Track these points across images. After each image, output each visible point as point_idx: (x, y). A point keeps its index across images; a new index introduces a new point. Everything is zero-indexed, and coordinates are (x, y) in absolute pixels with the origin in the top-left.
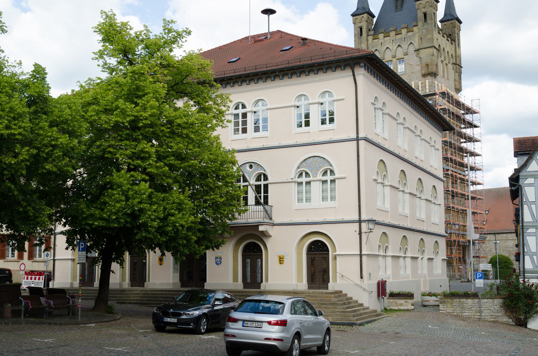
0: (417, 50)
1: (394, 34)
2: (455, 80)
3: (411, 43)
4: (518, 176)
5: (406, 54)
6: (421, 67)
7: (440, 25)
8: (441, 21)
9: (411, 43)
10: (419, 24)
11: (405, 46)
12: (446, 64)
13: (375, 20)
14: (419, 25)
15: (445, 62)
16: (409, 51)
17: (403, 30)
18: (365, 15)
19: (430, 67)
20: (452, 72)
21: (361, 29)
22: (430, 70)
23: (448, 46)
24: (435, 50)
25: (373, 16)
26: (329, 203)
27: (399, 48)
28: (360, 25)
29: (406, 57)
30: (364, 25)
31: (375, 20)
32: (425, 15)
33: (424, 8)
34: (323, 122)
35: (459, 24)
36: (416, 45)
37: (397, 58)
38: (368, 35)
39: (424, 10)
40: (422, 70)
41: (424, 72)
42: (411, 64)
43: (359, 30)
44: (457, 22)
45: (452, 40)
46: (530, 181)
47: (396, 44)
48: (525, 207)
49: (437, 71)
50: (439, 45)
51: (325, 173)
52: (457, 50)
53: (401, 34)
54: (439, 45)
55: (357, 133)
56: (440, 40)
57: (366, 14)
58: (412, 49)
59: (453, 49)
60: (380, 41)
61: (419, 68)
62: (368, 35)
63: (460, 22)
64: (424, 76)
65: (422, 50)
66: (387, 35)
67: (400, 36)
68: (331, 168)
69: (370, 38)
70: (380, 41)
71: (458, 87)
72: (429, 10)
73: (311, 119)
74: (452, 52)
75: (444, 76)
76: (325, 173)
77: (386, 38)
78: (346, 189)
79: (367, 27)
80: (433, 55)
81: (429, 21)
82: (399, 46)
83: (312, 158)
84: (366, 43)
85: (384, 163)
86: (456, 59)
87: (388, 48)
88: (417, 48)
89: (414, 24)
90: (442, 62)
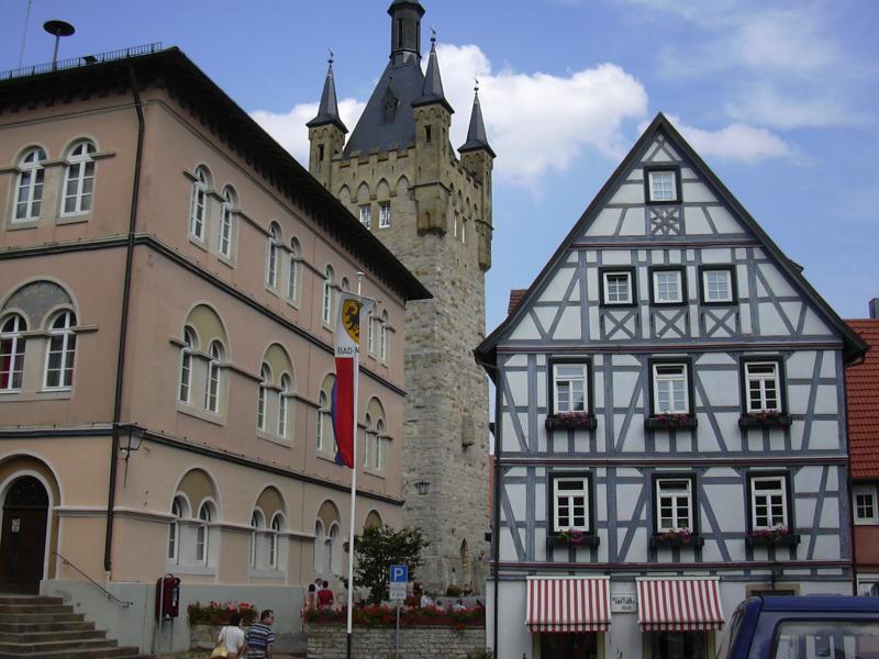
0: (412, 189)
1: (376, 160)
2: (479, 249)
3: (403, 176)
4: (495, 349)
5: (393, 195)
6: (418, 217)
7: (458, 156)
8: (460, 150)
9: (403, 176)
10: (418, 144)
12: (465, 220)
13: (347, 137)
14: (418, 147)
15: (461, 215)
17: (390, 154)
18: (330, 127)
20: (475, 235)
21: (322, 147)
22: (432, 224)
23: (468, 189)
24: (442, 191)
27: (383, 184)
29: (393, 200)
31: (347, 137)
32: (428, 129)
33: (427, 118)
35: (489, 157)
39: (427, 123)
40: (418, 222)
41: (421, 226)
43: (318, 150)
44: (486, 153)
46: (514, 361)
48: (506, 417)
49: (446, 227)
50: (452, 185)
52: (485, 197)
53: (386, 159)
54: (452, 185)
55: (133, 227)
57: (331, 125)
58: (403, 188)
59: (479, 196)
61: (414, 219)
62: (332, 161)
63: (494, 156)
64: (422, 232)
67: (385, 163)
68: (70, 307)
69: (336, 166)
71: (484, 261)
72: (432, 122)
75: (459, 238)
77: (362, 166)
78: (94, 355)
79: (332, 146)
80: (438, 198)
81: (433, 141)
83: (36, 286)
85: (379, 401)
86: (482, 212)
88: (412, 184)
89: (411, 144)
90: (456, 213)
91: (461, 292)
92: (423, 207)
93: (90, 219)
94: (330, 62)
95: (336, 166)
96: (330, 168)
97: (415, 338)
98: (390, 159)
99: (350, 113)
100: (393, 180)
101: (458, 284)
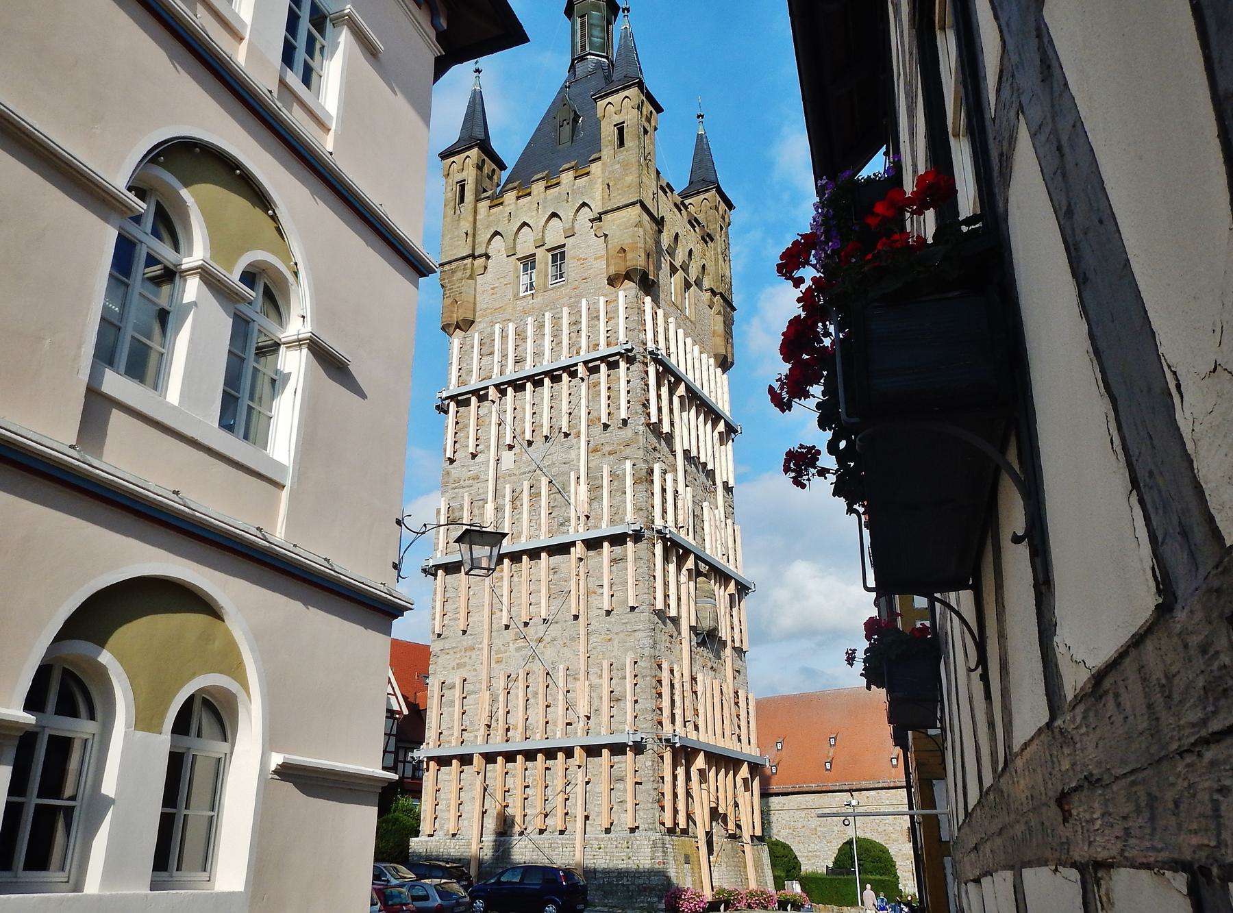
12: (688, 285)
16: (576, 226)
19: (629, 256)
25: (502, 167)
28: (459, 177)
30: (470, 175)
32: (621, 131)
36: (597, 207)
37: (547, 247)
38: (478, 200)
39: (617, 119)
40: (608, 266)
41: (612, 271)
42: (583, 256)
47: (544, 212)
57: (476, 150)
60: (508, 210)
62: (478, 200)
64: (612, 281)
70: (508, 210)
79: (478, 182)
84: (471, 219)
87: (525, 224)
90: (673, 270)
92: (615, 242)
95: (483, 206)
97: (606, 449)
98: (564, 182)
100: (567, 213)
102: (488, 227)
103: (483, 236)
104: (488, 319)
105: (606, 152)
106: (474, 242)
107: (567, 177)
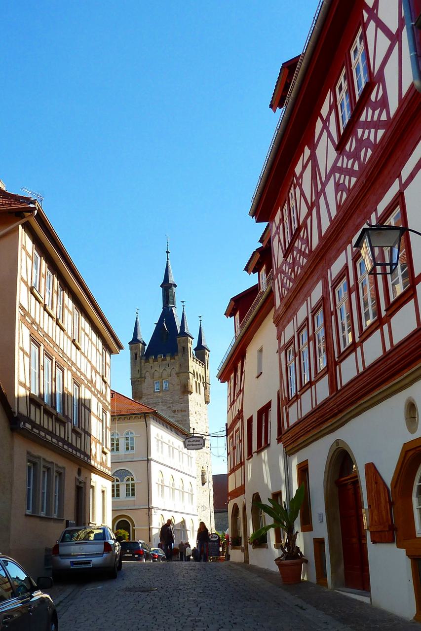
11: (168, 370)
20: (202, 388)
21: (136, 354)
23: (200, 370)
26: (131, 498)
27: (164, 372)
28: (135, 351)
31: (146, 347)
34: (127, 449)
38: (141, 359)
45: (203, 365)
51: (128, 480)
56: (194, 367)
58: (174, 373)
60: (151, 365)
63: (209, 351)
65: (181, 374)
66: (156, 360)
67: (165, 362)
69: (143, 361)
70: (151, 365)
73: (120, 447)
74: (203, 374)
76: (128, 480)
82: (164, 369)
84: (139, 366)
90: (196, 382)
91: (198, 416)
93: (135, 453)
94: (137, 313)
96: (141, 363)
99: (146, 336)
101: (197, 413)
102: (145, 369)
103: (144, 372)
104: (146, 397)
105: (180, 354)
106: (141, 374)
107: (168, 358)
